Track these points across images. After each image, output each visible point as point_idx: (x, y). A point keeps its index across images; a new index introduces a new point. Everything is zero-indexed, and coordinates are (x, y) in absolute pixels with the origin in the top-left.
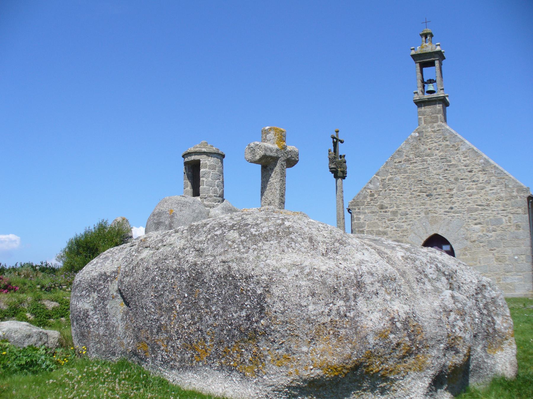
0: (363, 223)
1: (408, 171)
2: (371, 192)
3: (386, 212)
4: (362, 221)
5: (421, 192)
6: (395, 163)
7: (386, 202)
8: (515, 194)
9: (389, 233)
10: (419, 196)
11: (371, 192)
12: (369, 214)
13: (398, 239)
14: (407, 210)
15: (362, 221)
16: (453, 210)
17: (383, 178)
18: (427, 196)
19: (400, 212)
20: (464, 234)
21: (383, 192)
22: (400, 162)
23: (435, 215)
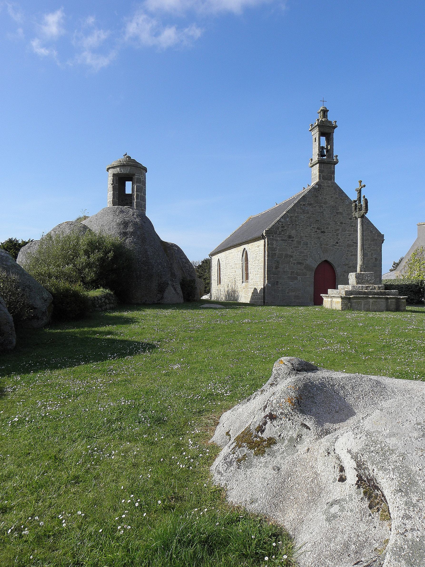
0: (276, 248)
1: (310, 213)
2: (282, 224)
3: (293, 241)
4: (274, 246)
5: (318, 228)
6: (301, 205)
7: (293, 232)
8: (376, 238)
9: (294, 256)
10: (316, 231)
11: (282, 224)
12: (281, 241)
13: (300, 261)
14: (308, 241)
15: (274, 246)
16: (338, 245)
17: (292, 215)
18: (322, 232)
19: (302, 242)
20: (344, 262)
21: (292, 225)
22: (304, 205)
23: (326, 246)
